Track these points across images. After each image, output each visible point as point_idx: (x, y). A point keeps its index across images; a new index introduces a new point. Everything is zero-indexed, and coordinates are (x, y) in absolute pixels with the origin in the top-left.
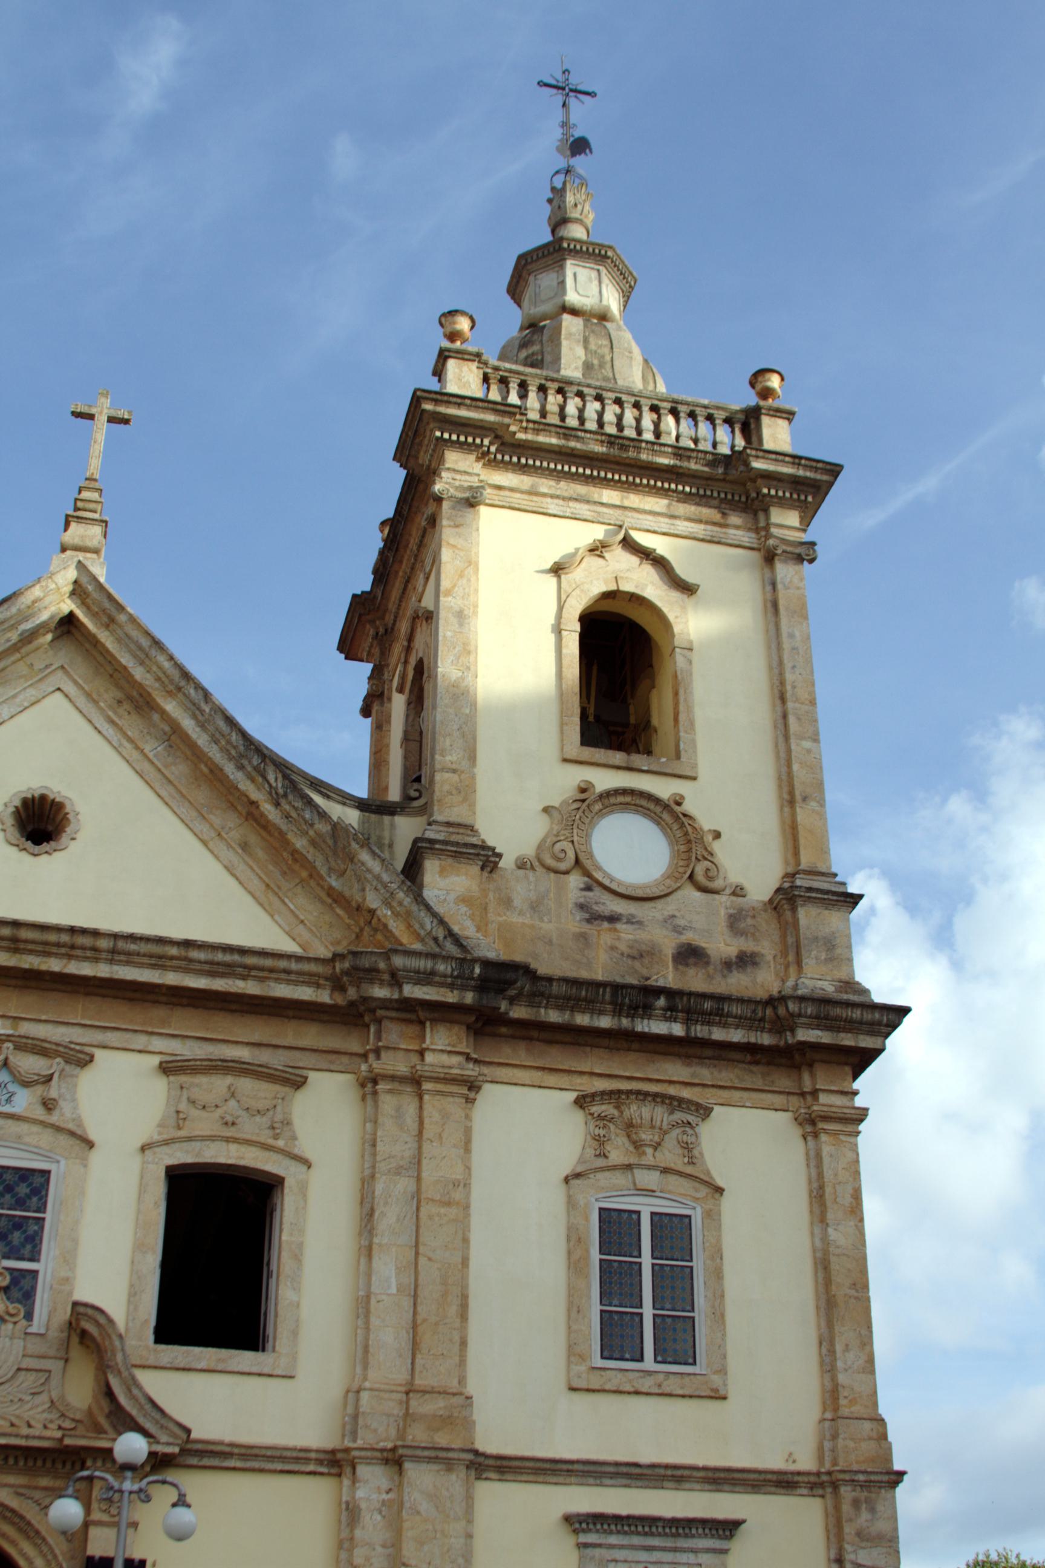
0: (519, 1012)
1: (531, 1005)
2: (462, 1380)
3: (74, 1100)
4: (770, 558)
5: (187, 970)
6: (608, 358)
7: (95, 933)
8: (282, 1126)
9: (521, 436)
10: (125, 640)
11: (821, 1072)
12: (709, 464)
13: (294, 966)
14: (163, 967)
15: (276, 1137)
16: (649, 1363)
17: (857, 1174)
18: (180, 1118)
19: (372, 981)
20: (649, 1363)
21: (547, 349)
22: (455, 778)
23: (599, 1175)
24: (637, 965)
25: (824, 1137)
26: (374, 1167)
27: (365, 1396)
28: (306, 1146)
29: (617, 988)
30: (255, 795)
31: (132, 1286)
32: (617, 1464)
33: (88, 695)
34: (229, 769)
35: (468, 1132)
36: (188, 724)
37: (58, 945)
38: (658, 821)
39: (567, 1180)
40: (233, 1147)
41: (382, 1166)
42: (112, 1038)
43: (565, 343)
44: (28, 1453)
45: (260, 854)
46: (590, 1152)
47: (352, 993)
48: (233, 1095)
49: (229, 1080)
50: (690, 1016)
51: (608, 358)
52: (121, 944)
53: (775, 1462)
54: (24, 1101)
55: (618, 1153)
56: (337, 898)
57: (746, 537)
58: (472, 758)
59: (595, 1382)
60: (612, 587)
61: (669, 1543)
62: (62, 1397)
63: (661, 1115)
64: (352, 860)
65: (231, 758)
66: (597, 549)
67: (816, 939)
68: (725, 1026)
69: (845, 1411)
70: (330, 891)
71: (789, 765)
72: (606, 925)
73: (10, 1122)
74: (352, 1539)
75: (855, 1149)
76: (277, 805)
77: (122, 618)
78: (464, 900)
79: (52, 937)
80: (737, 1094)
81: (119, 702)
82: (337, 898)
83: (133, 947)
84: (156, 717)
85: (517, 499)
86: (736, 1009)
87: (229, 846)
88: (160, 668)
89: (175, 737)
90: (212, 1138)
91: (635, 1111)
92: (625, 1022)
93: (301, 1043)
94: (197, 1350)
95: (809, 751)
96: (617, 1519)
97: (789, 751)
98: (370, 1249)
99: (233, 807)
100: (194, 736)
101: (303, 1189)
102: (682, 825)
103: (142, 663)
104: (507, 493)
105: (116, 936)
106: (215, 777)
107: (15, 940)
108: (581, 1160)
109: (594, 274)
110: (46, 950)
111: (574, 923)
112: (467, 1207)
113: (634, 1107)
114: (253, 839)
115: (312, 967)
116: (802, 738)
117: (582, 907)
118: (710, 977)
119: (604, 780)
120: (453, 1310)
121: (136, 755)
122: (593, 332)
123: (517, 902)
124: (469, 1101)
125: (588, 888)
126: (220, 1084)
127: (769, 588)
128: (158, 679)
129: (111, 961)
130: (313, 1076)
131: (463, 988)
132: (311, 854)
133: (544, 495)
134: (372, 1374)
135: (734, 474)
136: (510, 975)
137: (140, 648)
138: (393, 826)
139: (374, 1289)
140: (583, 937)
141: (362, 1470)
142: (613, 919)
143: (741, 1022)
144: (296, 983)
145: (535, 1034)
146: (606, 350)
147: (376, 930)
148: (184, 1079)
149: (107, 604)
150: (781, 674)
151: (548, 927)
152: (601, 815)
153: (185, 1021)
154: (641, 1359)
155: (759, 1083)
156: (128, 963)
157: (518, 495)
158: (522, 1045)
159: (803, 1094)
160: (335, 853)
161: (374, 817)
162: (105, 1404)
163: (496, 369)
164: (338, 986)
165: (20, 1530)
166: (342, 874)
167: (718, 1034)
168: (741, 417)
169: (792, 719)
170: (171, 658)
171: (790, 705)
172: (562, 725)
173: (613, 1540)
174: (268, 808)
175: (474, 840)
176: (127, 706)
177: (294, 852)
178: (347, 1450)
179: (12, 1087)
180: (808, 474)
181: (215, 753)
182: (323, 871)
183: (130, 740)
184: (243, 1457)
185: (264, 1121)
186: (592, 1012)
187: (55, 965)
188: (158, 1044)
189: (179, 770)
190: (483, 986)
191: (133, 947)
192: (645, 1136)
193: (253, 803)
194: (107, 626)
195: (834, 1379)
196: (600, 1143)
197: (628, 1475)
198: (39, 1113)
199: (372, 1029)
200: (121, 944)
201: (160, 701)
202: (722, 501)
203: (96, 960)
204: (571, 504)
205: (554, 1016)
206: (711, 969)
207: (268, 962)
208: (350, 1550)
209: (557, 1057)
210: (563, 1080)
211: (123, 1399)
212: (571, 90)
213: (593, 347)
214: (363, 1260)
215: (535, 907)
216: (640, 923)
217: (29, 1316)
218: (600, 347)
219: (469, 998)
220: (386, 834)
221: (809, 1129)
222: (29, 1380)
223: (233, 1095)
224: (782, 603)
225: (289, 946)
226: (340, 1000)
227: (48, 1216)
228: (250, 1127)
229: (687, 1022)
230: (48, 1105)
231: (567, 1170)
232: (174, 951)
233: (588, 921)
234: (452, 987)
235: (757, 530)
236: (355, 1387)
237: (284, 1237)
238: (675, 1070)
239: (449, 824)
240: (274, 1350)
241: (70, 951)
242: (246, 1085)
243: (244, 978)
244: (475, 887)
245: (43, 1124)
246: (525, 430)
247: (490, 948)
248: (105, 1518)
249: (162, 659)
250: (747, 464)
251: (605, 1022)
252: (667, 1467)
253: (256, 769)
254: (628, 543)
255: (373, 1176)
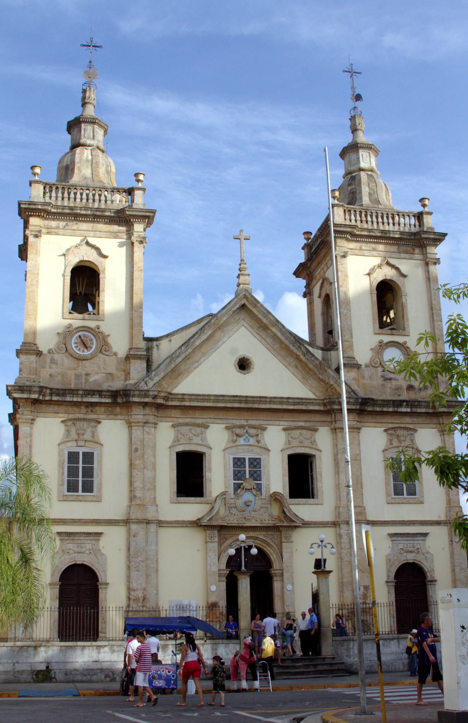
0: (369, 409)
1: (373, 407)
2: (363, 503)
3: (264, 439)
4: (427, 264)
5: (288, 404)
6: (375, 190)
7: (266, 397)
8: (314, 442)
9: (357, 233)
10: (259, 311)
11: (444, 417)
12: (409, 236)
13: (314, 401)
14: (282, 404)
15: (312, 445)
16: (405, 496)
17: (454, 445)
18: (289, 442)
19: (334, 404)
20: (405, 496)
21: (357, 188)
22: (348, 343)
23: (391, 449)
24: (397, 391)
25: (446, 436)
26: (337, 451)
27: (341, 508)
28: (320, 446)
29: (394, 401)
30: (299, 354)
31: (283, 485)
32: (399, 521)
33: (251, 327)
34: (291, 346)
35: (359, 440)
36: (279, 334)
37: (257, 401)
38: (400, 349)
39: (383, 451)
40: (303, 448)
41: (339, 451)
42: (270, 422)
43: (363, 186)
44: (267, 527)
45: (300, 368)
46: (388, 443)
47: (329, 407)
48: (301, 435)
49: (300, 431)
50: (412, 406)
51: (375, 190)
52: (272, 400)
53: (435, 518)
54: (252, 441)
55: (395, 444)
56: (321, 380)
57: (420, 257)
58: (352, 336)
59: (393, 501)
60: (384, 278)
61: (412, 539)
62: (271, 513)
63: (405, 432)
64: (326, 371)
65: (291, 344)
66: (380, 266)
67: (443, 381)
68: (420, 408)
69: (452, 505)
70: (319, 378)
71: (434, 329)
72: (389, 381)
73: (250, 447)
74: (341, 542)
75: (453, 438)
76: (304, 356)
77: (259, 305)
78: (354, 379)
79: (255, 399)
80: (424, 425)
81: (259, 327)
82: (321, 380)
83: (275, 400)
84: (269, 331)
85: (357, 252)
86: (423, 404)
87: (292, 367)
88: (270, 319)
89: (274, 337)
90: (298, 447)
91: (400, 432)
92: (396, 409)
93: (316, 420)
94: (300, 499)
95: (439, 325)
96: (400, 534)
97: (434, 325)
98: (338, 472)
99: (292, 356)
100: (281, 338)
101: (320, 458)
102: (407, 350)
103: (265, 317)
104: (354, 250)
105: (271, 398)
106: (287, 348)
107: (246, 401)
108: (386, 446)
109: (368, 154)
110: (254, 402)
111: (380, 381)
112: (360, 460)
113: (399, 431)
114: (298, 364)
115: (319, 401)
116: (438, 321)
117: (382, 376)
118: (415, 393)
119: (386, 339)
120: (360, 486)
121: (265, 343)
122: (370, 181)
123: (366, 377)
124: (359, 433)
125: (384, 371)
126: (298, 432)
127: (427, 273)
128: (270, 322)
129: (270, 404)
130: (320, 428)
131: (357, 405)
132: (314, 369)
133: (364, 250)
134: (342, 503)
135: (416, 238)
136: (368, 401)
137: (265, 314)
138: (330, 354)
139: (341, 482)
140: (383, 385)
141: (342, 526)
142: (390, 379)
143: (425, 407)
144: (314, 405)
145: (373, 413)
146: (375, 187)
147: (332, 389)
148: (289, 432)
149: (254, 301)
150: (431, 301)
151: (374, 383)
152: (385, 349)
153: (287, 416)
154: (403, 495)
155: (429, 422)
156: (274, 404)
157: (357, 251)
158: (370, 416)
159: (440, 424)
160: (320, 369)
161: (325, 352)
162: (283, 514)
163: (347, 208)
164: (325, 405)
165: (267, 545)
166: (323, 374)
167: (419, 410)
168: (417, 215)
169: (435, 316)
170: (273, 316)
171: (434, 311)
172: (374, 323)
173: (399, 539)
174: (302, 357)
175: (355, 362)
176: (261, 328)
177: (309, 368)
178: (338, 522)
179: (249, 438)
180: (438, 237)
181: (286, 342)
182: (318, 374)
183: (263, 339)
184: (314, 524)
185: (309, 441)
186: (387, 407)
187: (256, 406)
188: (282, 423)
189: (277, 346)
190: (361, 404)
191: (275, 400)
192: (402, 439)
193: (299, 356)
194: (254, 307)
195: (449, 497)
196: (391, 441)
197: (402, 523)
198: (256, 444)
199: (333, 415)
200: (272, 400)
201: (271, 328)
202: (414, 245)
203: (266, 404)
204: (372, 252)
205: (378, 409)
206: (416, 391)
207: (308, 401)
208: (341, 544)
209: (379, 419)
210: (381, 425)
211: (288, 514)
212: (354, 72)
213: (371, 187)
214: (337, 475)
215: (371, 378)
216: (397, 380)
217: (261, 495)
218: (373, 186)
219: (358, 407)
220: (329, 357)
221: (442, 433)
222: (263, 510)
223: (301, 435)
224: (431, 279)
225: (311, 396)
226: (325, 409)
227: (262, 469)
228: (307, 443)
229: (411, 408)
230: (258, 442)
231: (383, 448)
232: (285, 400)
233: (384, 380)
234: (354, 405)
235: (423, 254)
236: (338, 506)
237: (317, 470)
238: (408, 419)
239: (348, 357)
240: (317, 498)
241: (260, 402)
242: (304, 432)
243: (302, 405)
244: (356, 375)
245: (258, 446)
246: (358, 231)
247: (362, 394)
248: (286, 541)
249: (270, 316)
250: (420, 235)
251: (391, 410)
252: (411, 521)
253: (298, 347)
254: (388, 264)
255: (337, 454)
